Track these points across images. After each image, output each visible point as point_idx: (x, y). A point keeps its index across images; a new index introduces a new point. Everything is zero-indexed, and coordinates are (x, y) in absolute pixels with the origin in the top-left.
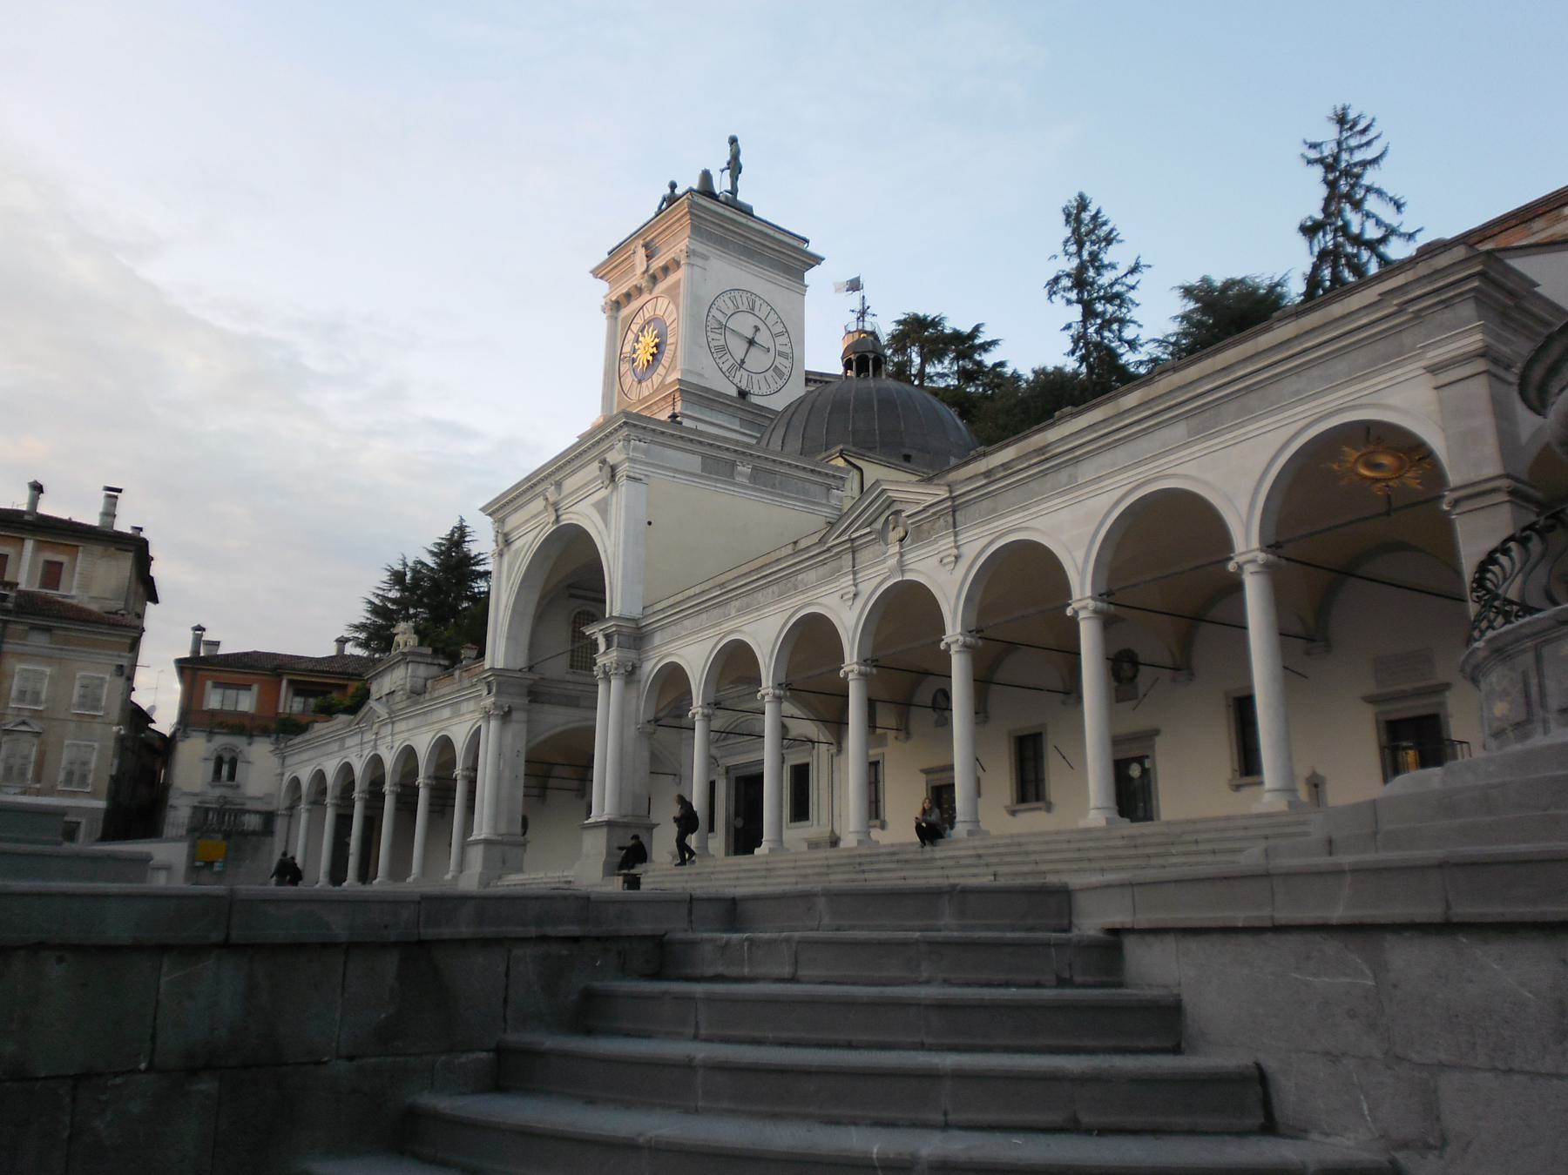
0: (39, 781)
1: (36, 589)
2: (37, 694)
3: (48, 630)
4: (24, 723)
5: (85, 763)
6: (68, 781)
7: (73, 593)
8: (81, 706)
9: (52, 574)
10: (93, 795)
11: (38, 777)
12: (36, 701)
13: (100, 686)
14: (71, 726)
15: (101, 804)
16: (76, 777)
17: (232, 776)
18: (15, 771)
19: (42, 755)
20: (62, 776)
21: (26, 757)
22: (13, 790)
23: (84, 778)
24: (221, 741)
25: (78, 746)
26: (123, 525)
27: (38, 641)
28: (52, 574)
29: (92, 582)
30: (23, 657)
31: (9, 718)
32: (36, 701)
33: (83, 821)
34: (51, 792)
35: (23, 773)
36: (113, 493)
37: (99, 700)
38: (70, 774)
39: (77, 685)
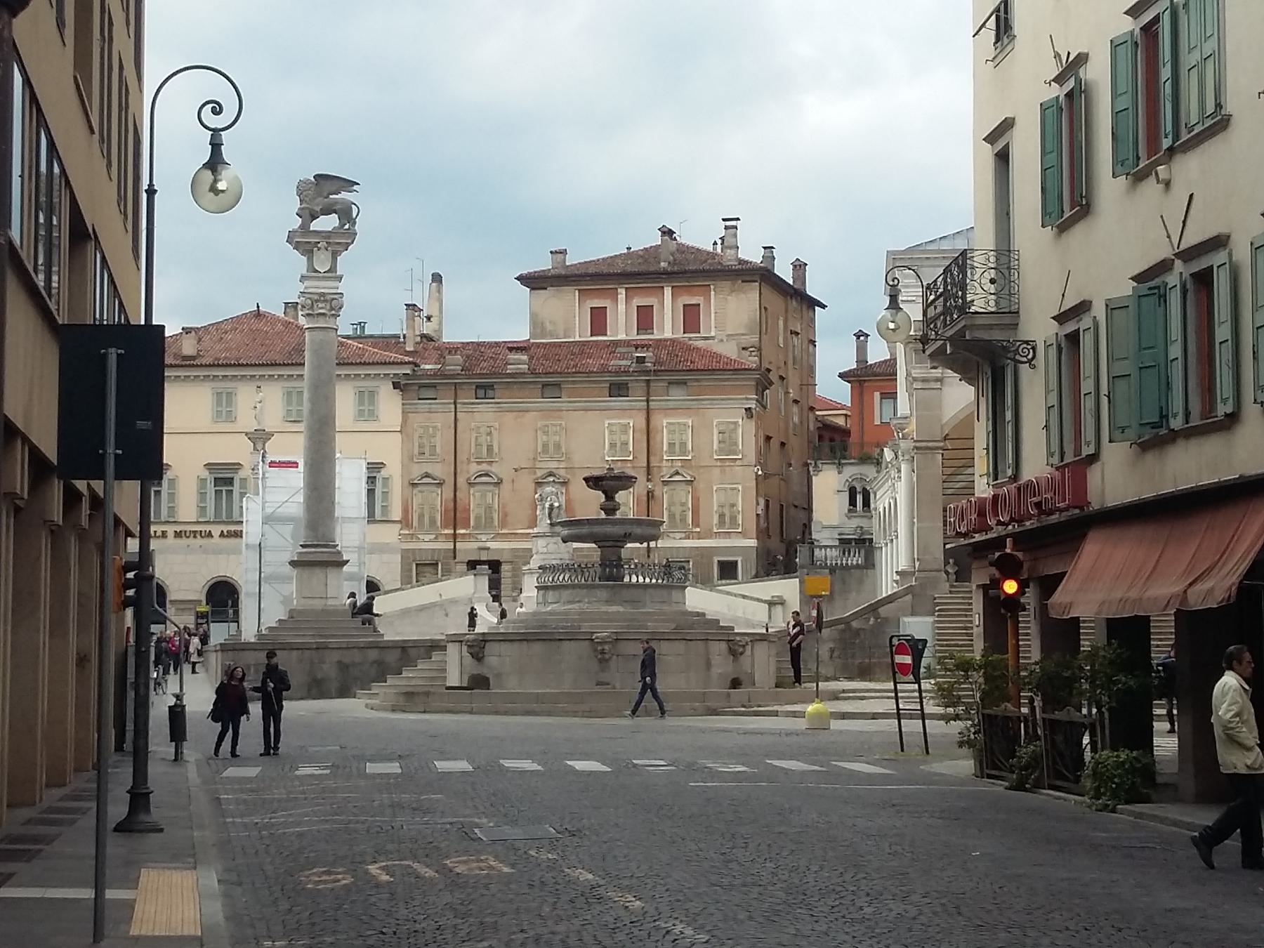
0: (698, 526)
1: (680, 335)
2: (683, 444)
3: (684, 383)
4: (677, 473)
5: (733, 505)
6: (722, 522)
7: (713, 334)
8: (721, 451)
9: (691, 318)
10: (743, 534)
11: (696, 523)
12: (684, 453)
13: (735, 430)
14: (717, 471)
15: (753, 543)
16: (727, 519)
17: (866, 503)
18: (678, 517)
19: (696, 501)
20: (716, 520)
21: (683, 504)
22: (678, 536)
23: (733, 519)
24: (850, 471)
25: (725, 489)
26: (751, 253)
27: (677, 394)
28: (691, 318)
29: (729, 319)
30: (667, 411)
31: (665, 471)
32: (684, 453)
33: (740, 560)
34: (709, 534)
35: (683, 520)
36: (731, 224)
37: (736, 444)
38: (722, 516)
39: (715, 432)
